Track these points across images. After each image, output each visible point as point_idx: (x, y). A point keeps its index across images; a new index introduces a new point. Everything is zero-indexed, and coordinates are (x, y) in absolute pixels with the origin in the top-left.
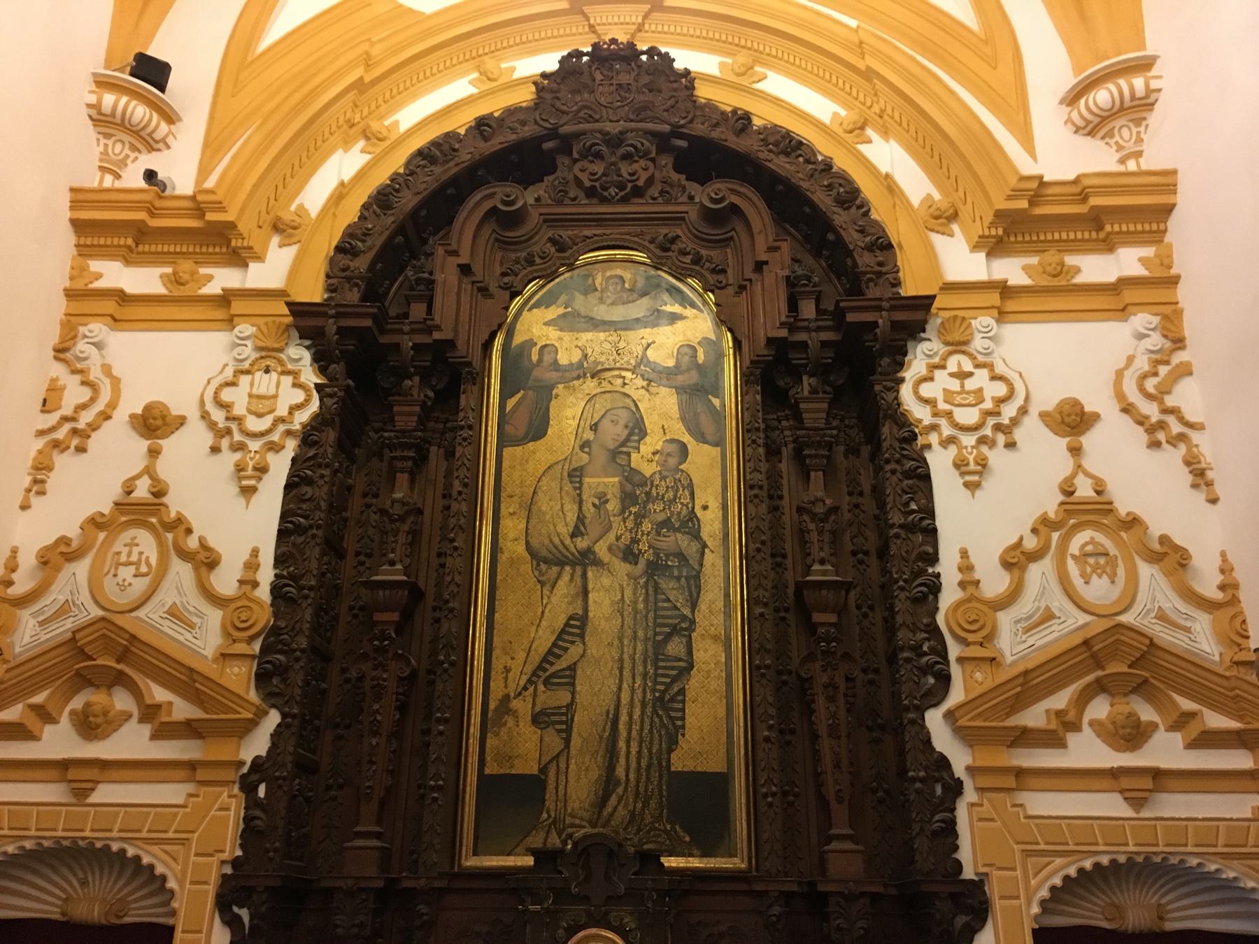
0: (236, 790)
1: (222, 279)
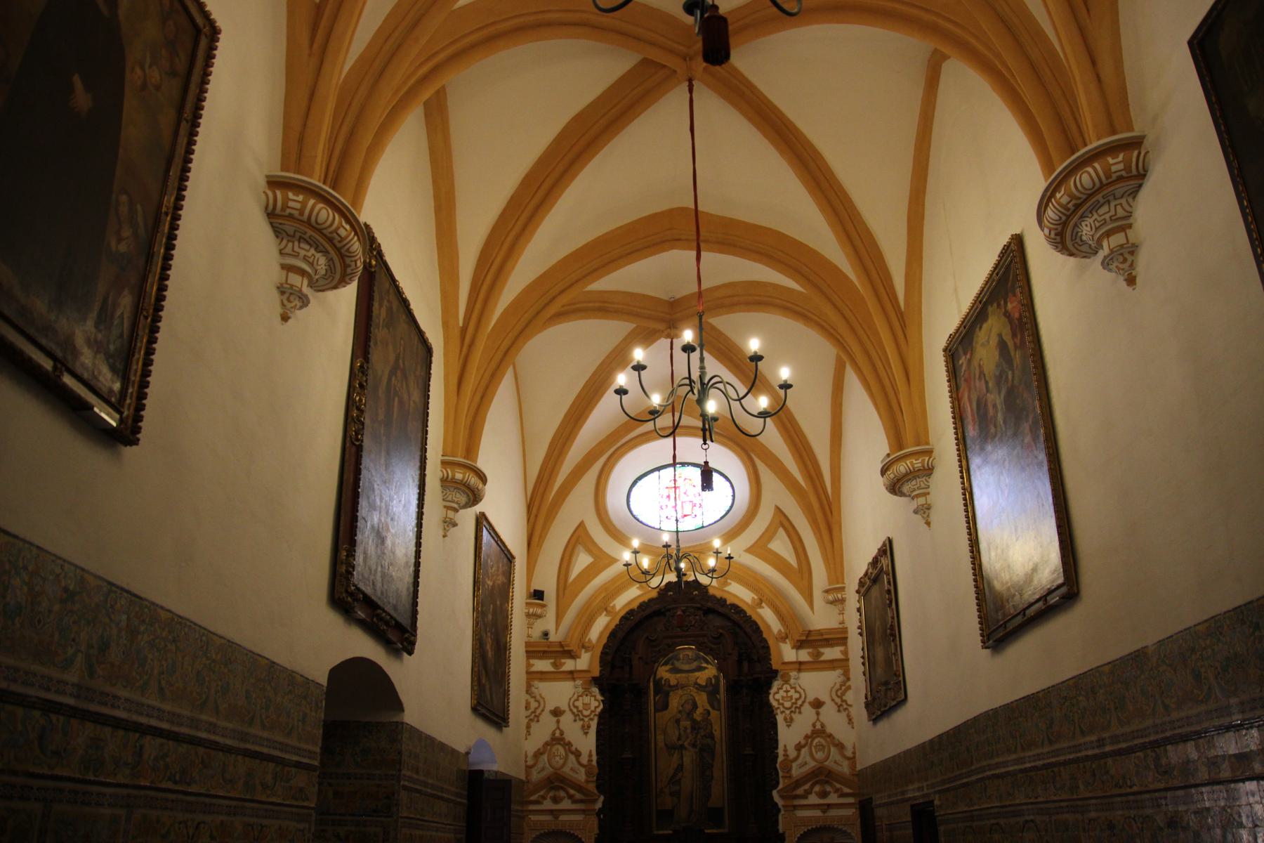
1: (569, 665)
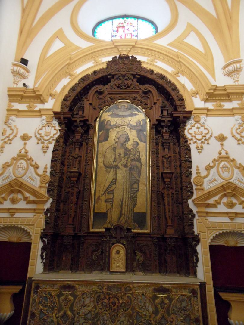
0: (44, 214)
1: (39, 106)
